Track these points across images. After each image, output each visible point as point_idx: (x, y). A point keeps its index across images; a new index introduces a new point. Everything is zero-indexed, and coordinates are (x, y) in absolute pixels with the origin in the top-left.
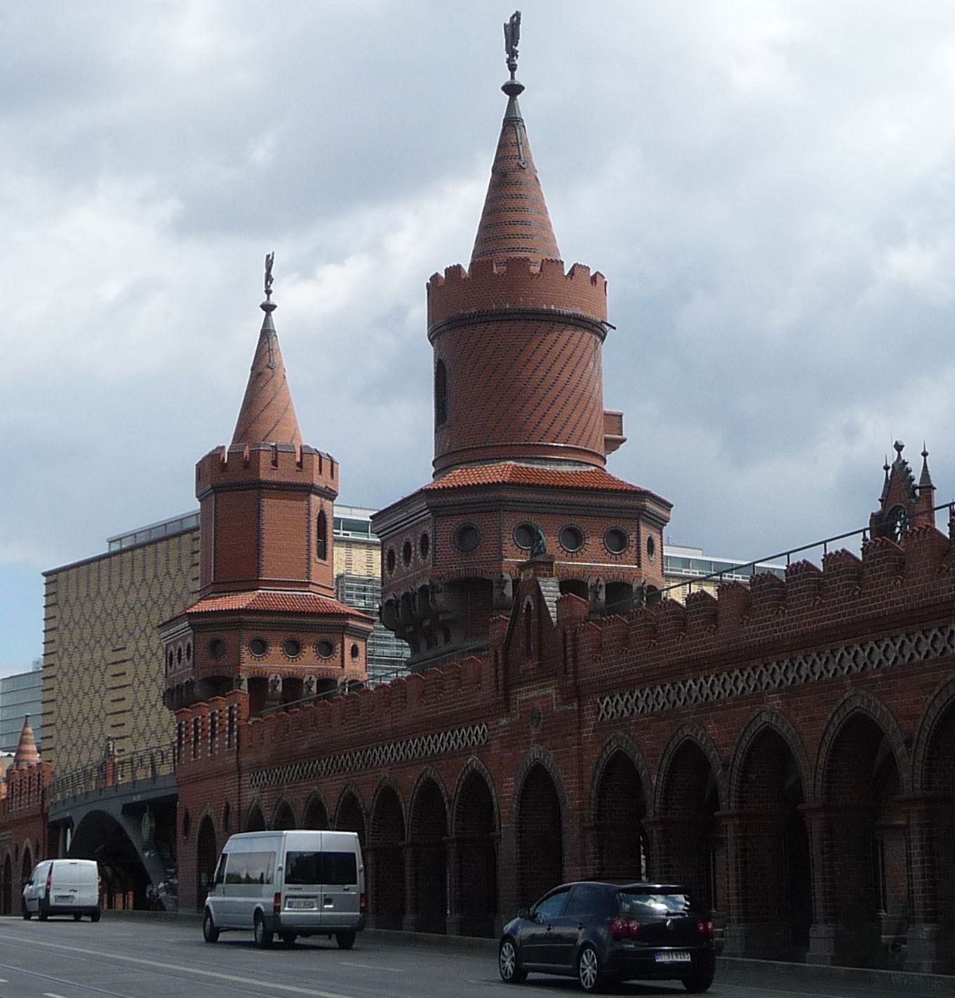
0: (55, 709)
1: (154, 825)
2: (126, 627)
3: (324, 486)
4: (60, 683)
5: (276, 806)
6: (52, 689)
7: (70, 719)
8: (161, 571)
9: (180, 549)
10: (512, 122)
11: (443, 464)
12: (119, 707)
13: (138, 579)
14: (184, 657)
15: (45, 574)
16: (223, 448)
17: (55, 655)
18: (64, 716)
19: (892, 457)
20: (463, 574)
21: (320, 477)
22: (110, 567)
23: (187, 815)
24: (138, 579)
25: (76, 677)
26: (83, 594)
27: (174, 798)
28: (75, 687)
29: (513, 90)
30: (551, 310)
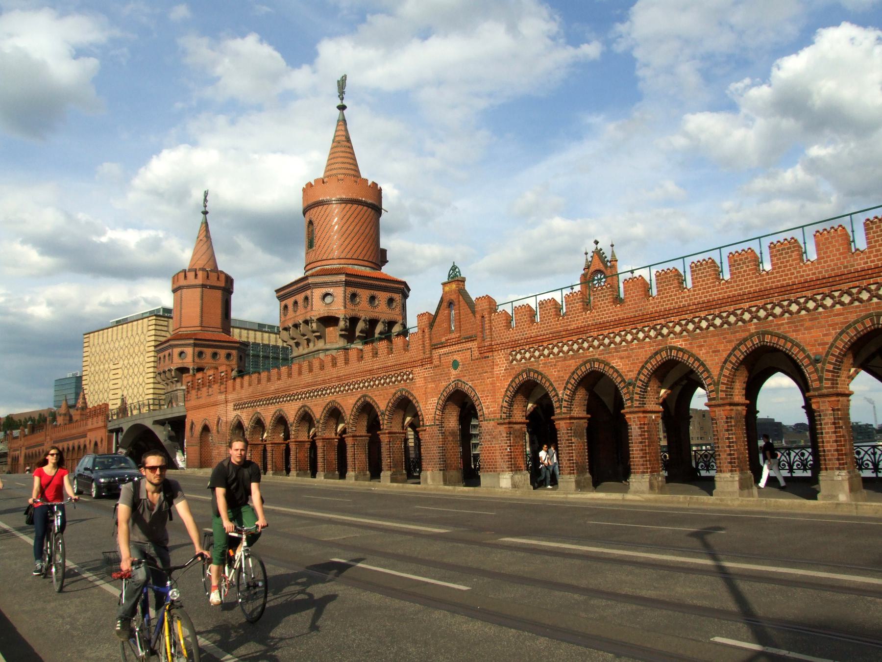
2: (119, 355)
4: (90, 377)
5: (251, 419)
8: (134, 333)
9: (143, 324)
12: (116, 387)
13: (124, 336)
19: (593, 247)
20: (326, 315)
22: (112, 331)
23: (192, 423)
24: (124, 336)
25: (97, 375)
27: (184, 417)
28: (97, 379)
29: (342, 108)
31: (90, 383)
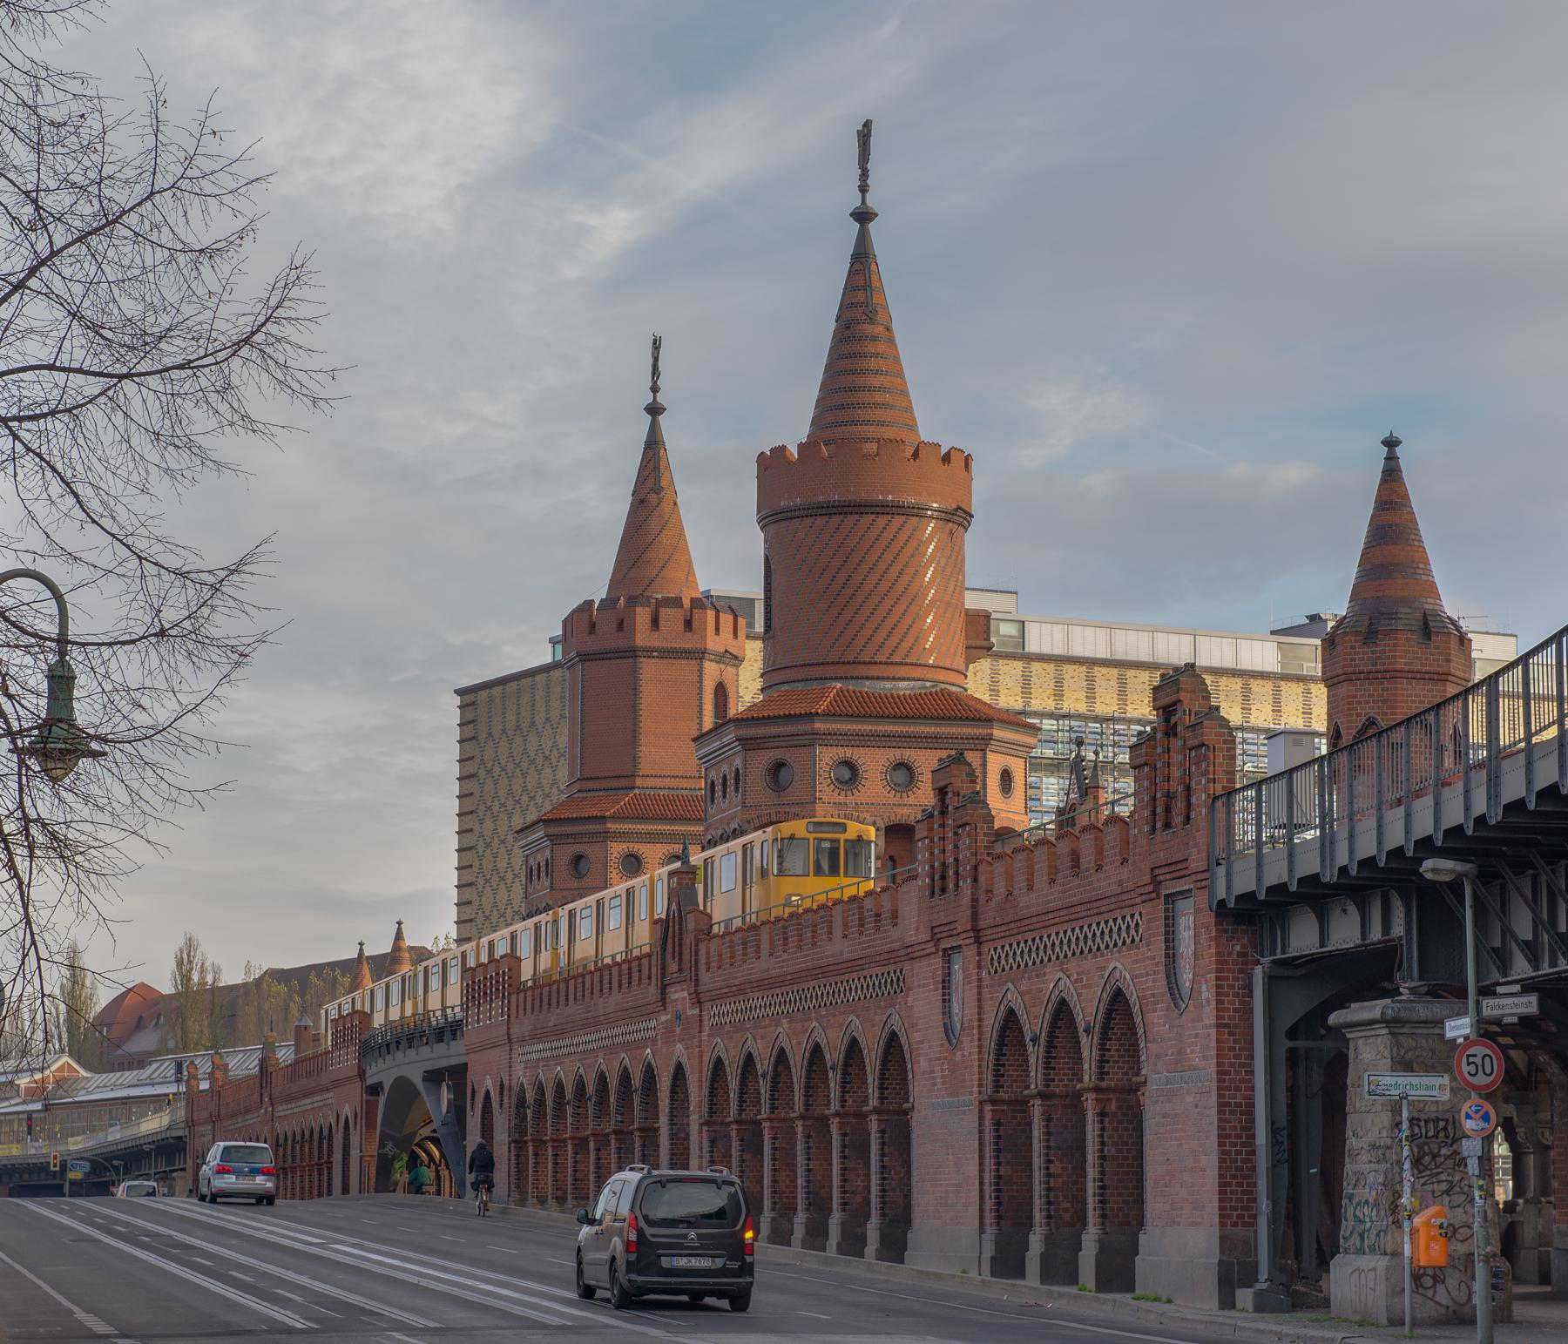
0: (474, 897)
1: (452, 1096)
3: (722, 650)
6: (471, 866)
7: (495, 912)
10: (862, 258)
11: (775, 677)
14: (543, 874)
15: (459, 692)
16: (592, 602)
17: (474, 815)
18: (487, 908)
21: (717, 638)
25: (502, 850)
26: (511, 726)
27: (466, 1064)
28: (502, 865)
30: (887, 501)
31: (481, 882)
